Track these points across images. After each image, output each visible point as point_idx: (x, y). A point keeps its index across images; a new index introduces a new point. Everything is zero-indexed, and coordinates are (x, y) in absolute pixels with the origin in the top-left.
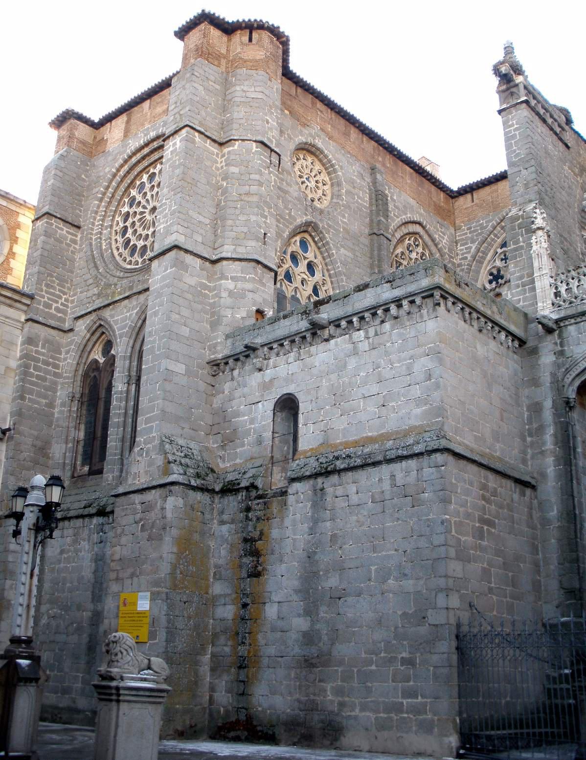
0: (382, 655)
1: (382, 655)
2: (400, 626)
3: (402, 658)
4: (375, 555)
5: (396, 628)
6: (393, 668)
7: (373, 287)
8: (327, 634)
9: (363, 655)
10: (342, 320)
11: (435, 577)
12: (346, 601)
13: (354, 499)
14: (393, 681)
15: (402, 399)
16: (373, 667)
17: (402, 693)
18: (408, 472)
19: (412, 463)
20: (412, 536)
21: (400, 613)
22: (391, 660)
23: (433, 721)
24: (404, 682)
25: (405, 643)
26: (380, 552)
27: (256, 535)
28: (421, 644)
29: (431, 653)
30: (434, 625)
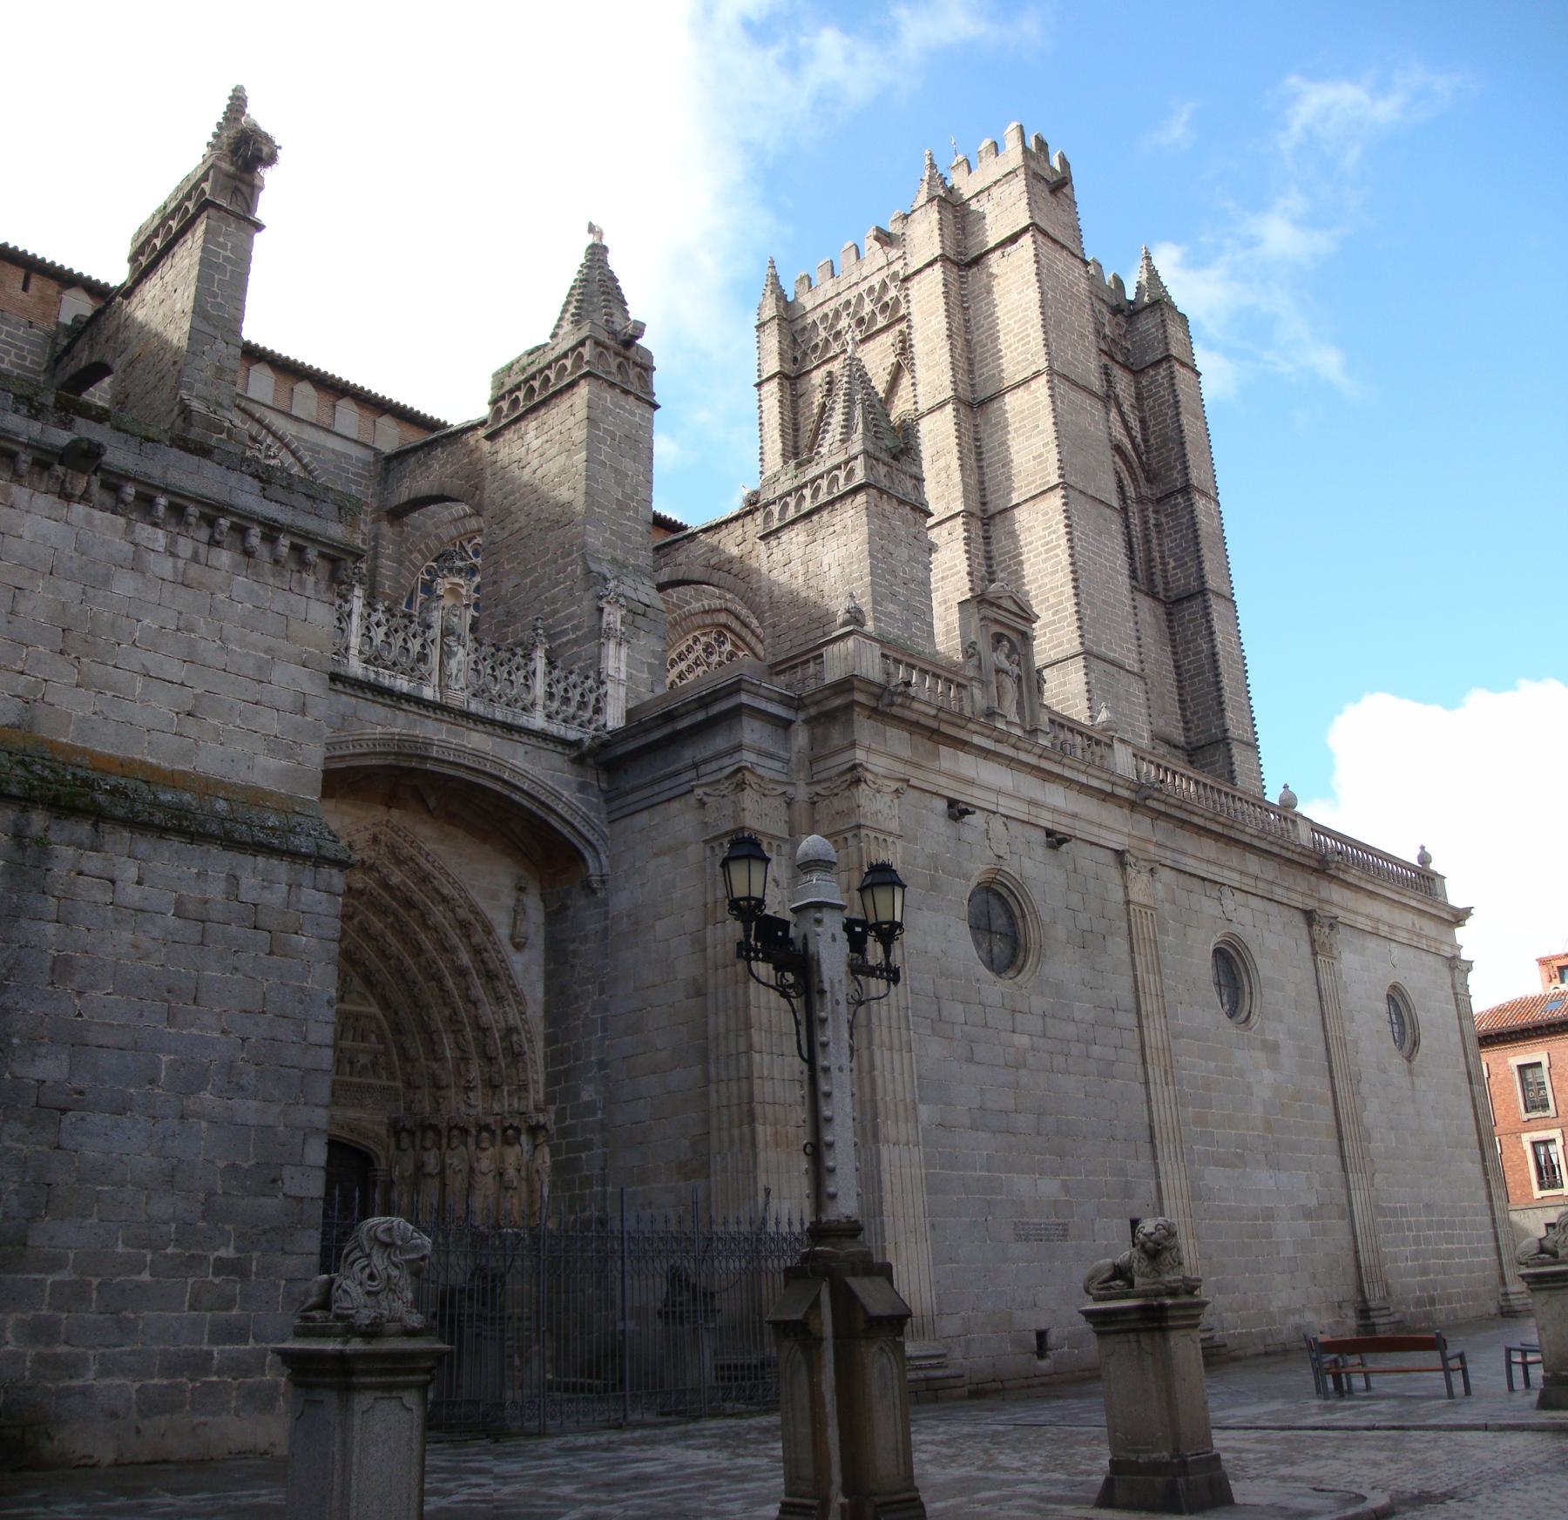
0: (170, 1250)
1: (170, 1250)
2: (220, 1192)
3: (219, 1258)
4: (173, 1030)
5: (210, 1194)
6: (194, 1279)
7: (220, 464)
8: (17, 1192)
9: (120, 1249)
10: (130, 484)
11: (305, 1104)
12: (83, 1119)
13: (131, 894)
14: (192, 1308)
15: (238, 722)
16: (145, 1277)
18: (268, 883)
19: (281, 869)
20: (263, 1012)
21: (221, 1164)
24: (220, 1309)
25: (228, 1227)
28: (265, 1232)
29: (285, 1253)
30: (295, 1198)
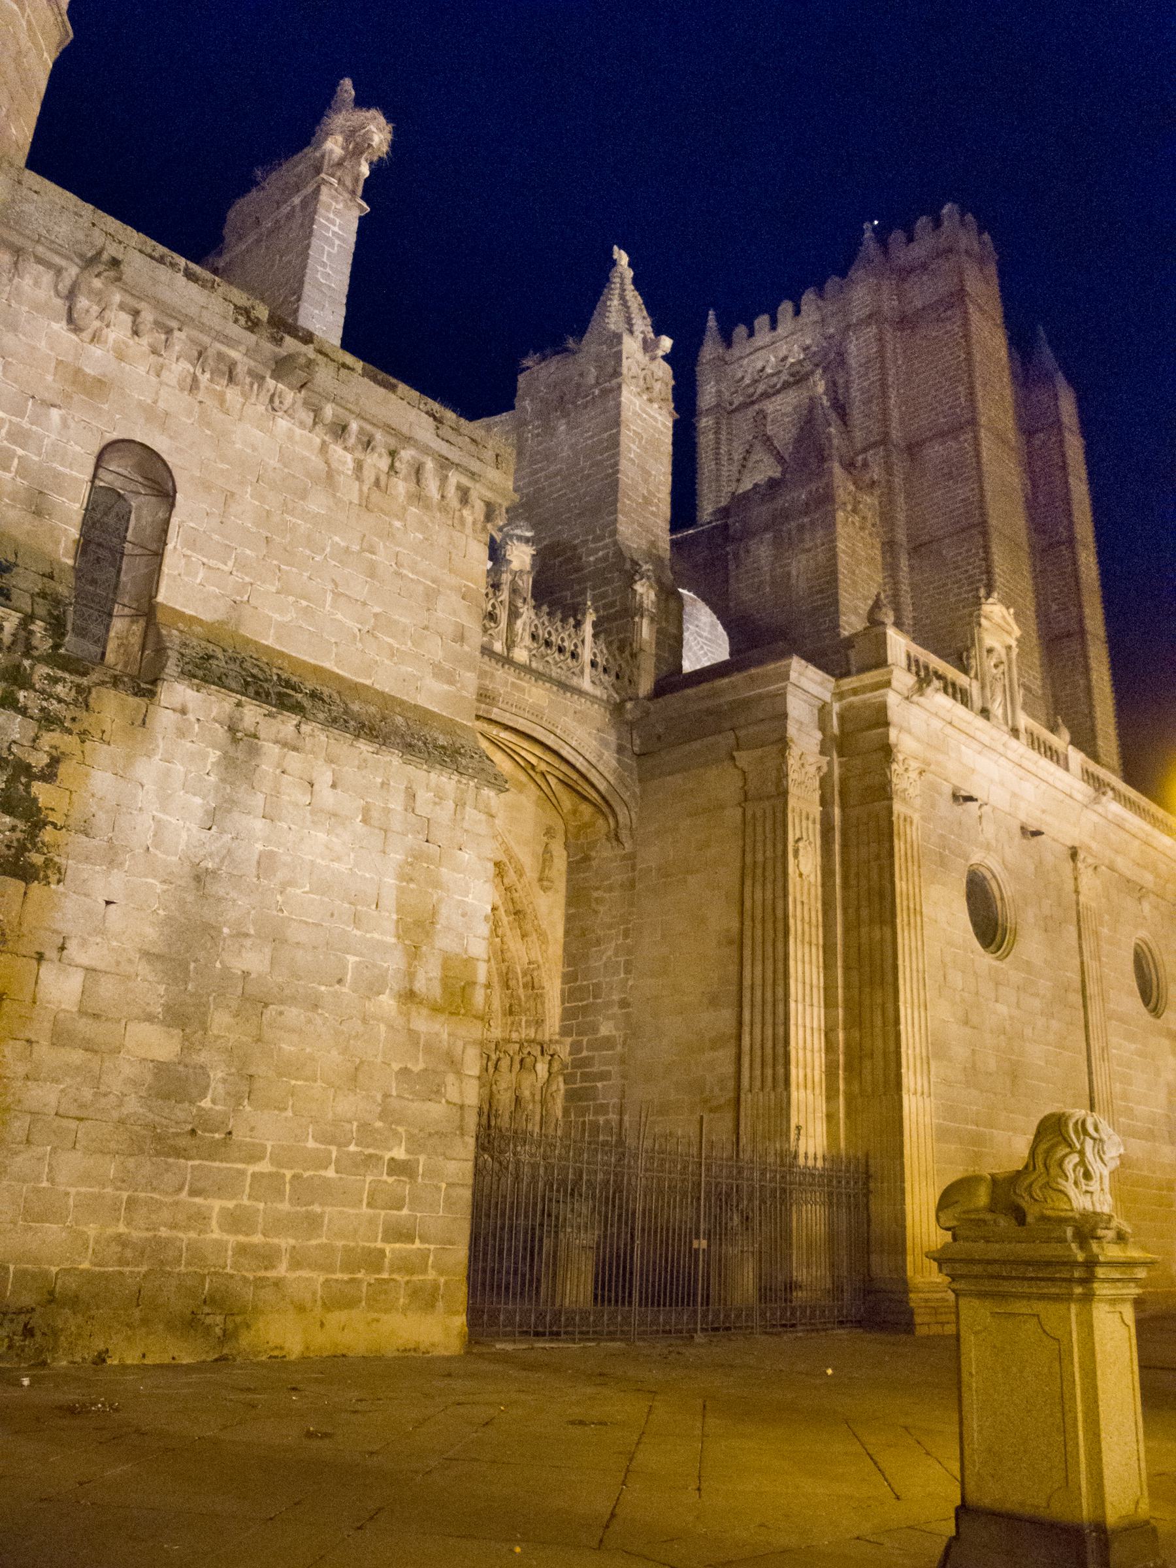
0: (352, 1148)
1: (352, 1148)
4: (358, 933)
5: (386, 1096)
8: (224, 1081)
9: (311, 1144)
14: (369, 1205)
16: (331, 1173)
17: (385, 1232)
21: (396, 1066)
22: (370, 1161)
23: (436, 1287)
25: (401, 1129)
26: (367, 932)
27: (39, 760)
